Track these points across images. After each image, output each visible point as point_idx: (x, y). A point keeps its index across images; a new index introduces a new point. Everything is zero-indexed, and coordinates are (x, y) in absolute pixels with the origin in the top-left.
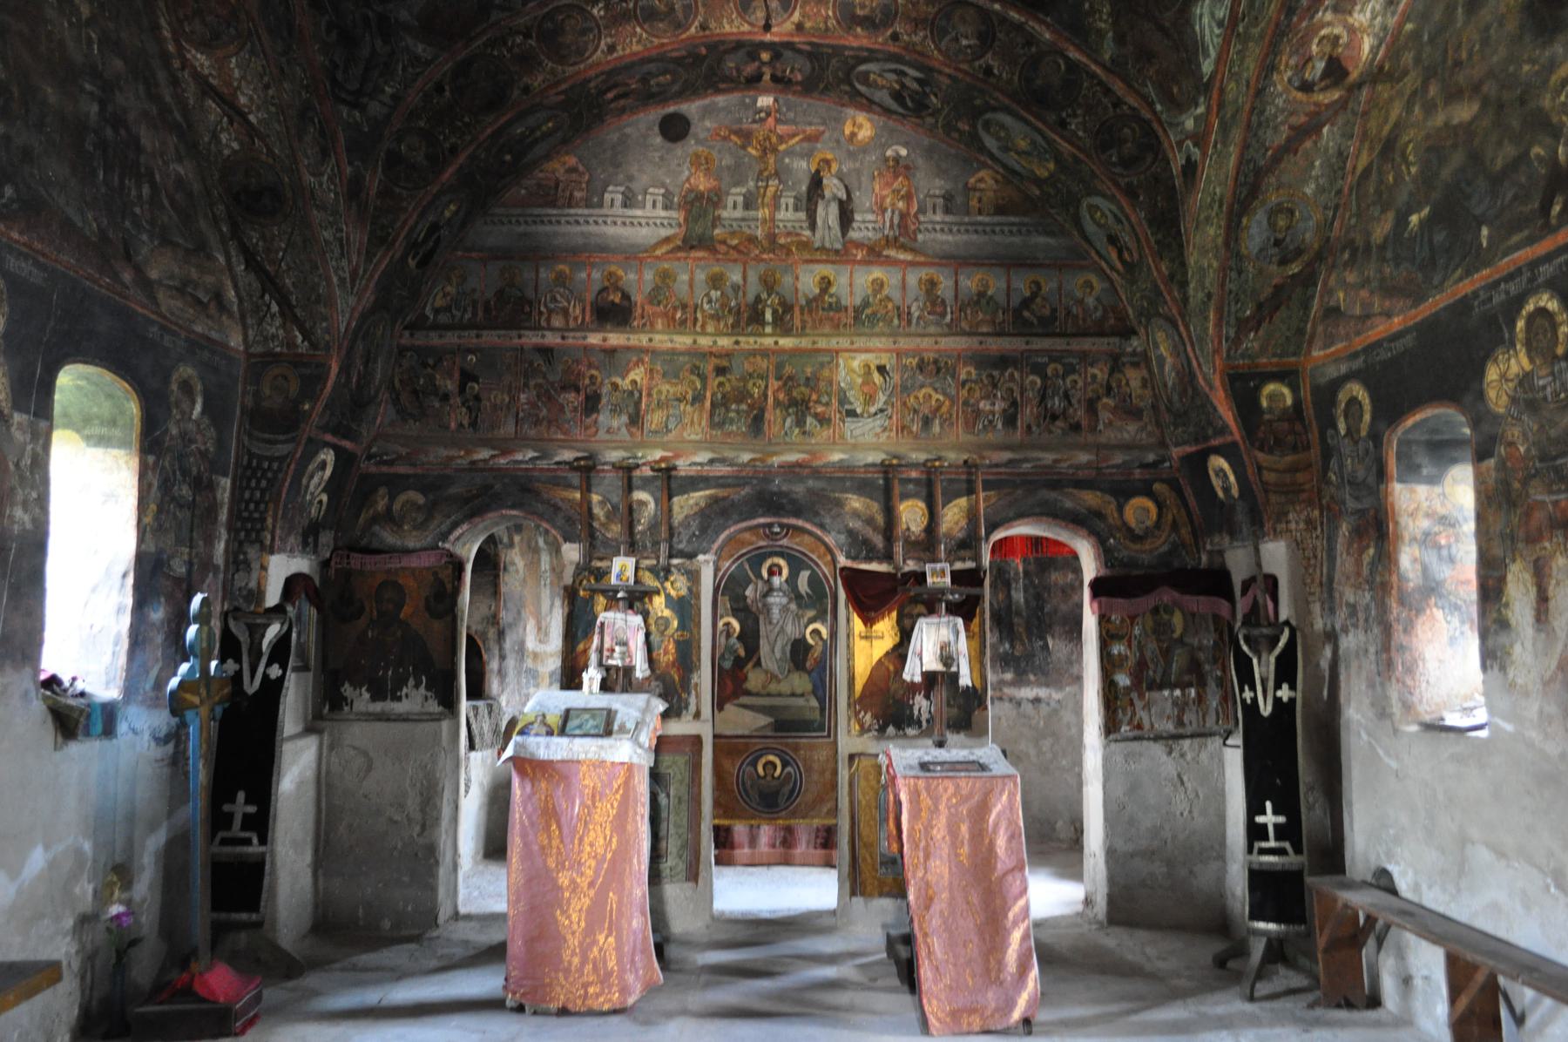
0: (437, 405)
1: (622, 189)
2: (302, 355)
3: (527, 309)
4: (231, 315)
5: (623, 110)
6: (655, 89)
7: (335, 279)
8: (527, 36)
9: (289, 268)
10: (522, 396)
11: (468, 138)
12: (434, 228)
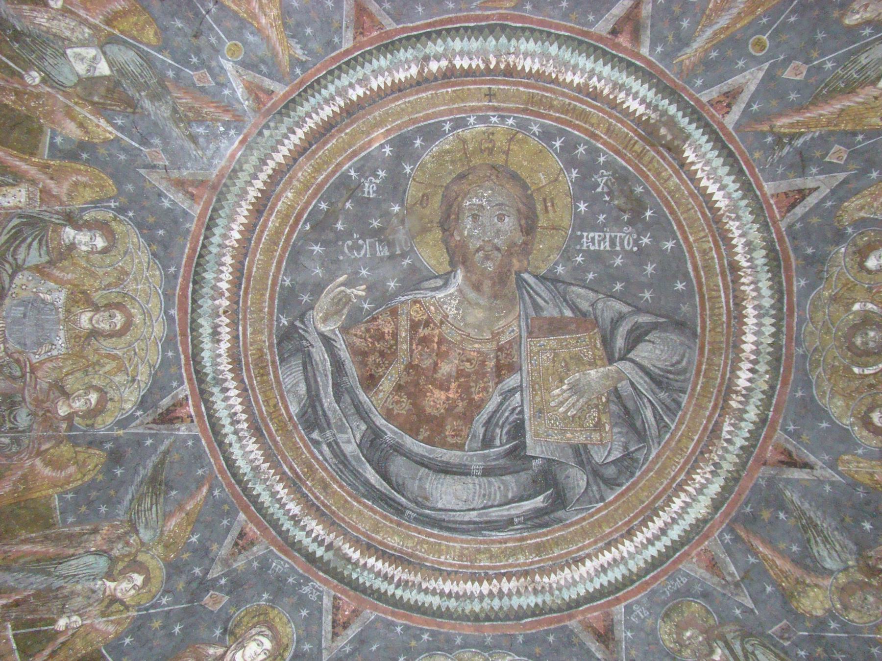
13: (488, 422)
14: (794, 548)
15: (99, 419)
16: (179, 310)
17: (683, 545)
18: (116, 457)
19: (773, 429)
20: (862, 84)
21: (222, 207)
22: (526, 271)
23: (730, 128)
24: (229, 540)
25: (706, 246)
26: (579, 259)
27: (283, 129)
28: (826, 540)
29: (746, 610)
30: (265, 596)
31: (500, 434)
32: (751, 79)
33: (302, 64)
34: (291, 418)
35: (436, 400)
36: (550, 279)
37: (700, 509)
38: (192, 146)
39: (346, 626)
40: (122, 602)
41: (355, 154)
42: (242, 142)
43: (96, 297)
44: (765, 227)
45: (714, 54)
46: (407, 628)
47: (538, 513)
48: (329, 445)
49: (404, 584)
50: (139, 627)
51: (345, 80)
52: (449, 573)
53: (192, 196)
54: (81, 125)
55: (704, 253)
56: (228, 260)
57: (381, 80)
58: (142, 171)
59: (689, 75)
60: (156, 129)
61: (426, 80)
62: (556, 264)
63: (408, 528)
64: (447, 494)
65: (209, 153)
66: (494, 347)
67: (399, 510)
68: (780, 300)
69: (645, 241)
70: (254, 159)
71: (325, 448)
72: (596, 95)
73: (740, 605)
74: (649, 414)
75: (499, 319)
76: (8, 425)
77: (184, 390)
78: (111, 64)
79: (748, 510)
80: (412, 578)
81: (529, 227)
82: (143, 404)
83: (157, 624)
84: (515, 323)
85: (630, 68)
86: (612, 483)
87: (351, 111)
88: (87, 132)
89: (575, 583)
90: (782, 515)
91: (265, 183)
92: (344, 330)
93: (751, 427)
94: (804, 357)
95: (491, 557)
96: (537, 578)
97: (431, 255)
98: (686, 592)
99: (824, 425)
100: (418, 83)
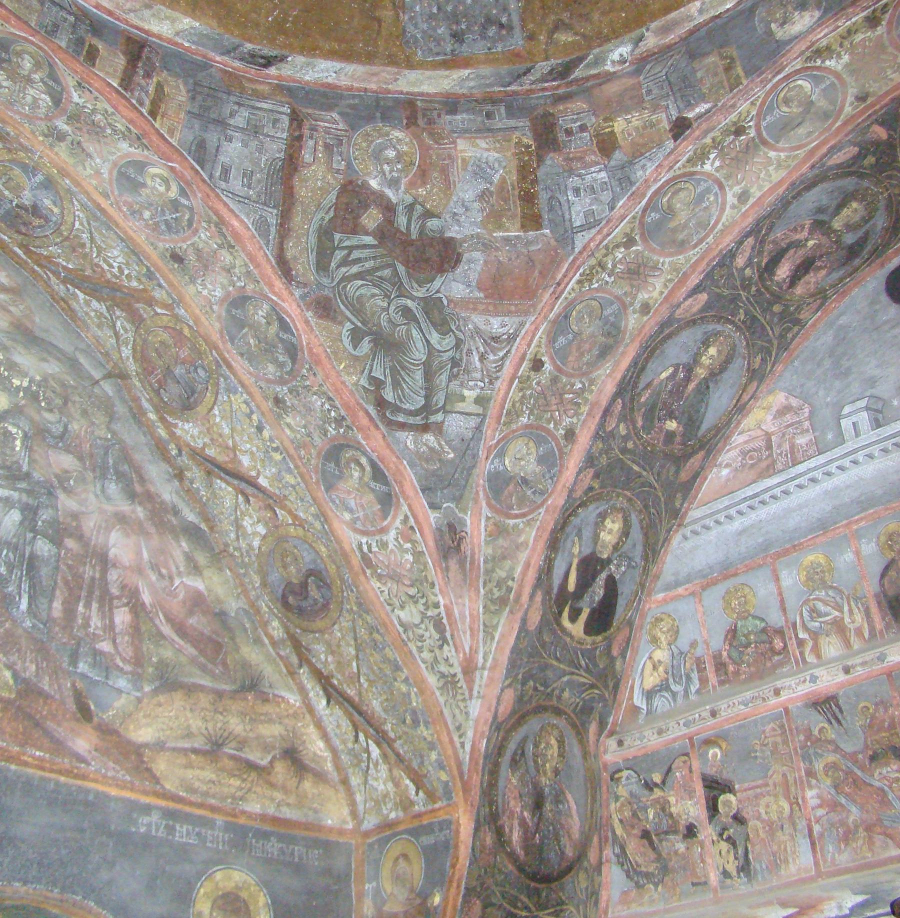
0: (681, 847)
1: (863, 403)
2: (419, 815)
3: (778, 644)
4: (320, 777)
5: (821, 296)
6: (849, 239)
7: (432, 680)
8: (630, 242)
9: (371, 682)
10: (810, 794)
11: (585, 409)
12: (590, 566)
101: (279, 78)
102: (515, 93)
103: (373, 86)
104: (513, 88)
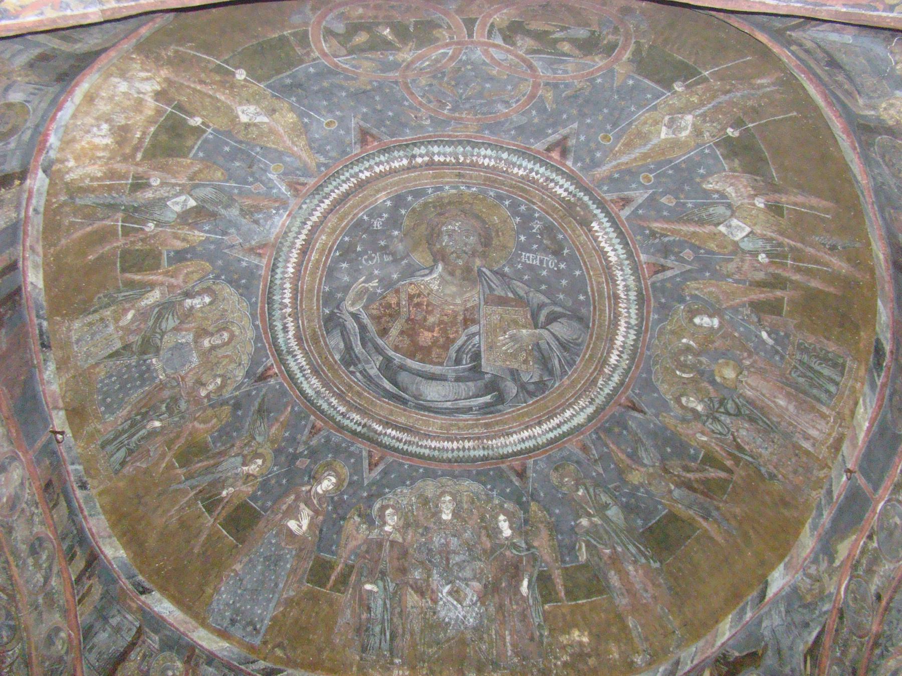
13: (458, 351)
14: (629, 450)
15: (224, 390)
16: (261, 321)
17: (569, 435)
18: (237, 406)
19: (627, 389)
20: (710, 223)
21: (280, 256)
22: (484, 266)
23: (623, 218)
24: (306, 431)
25: (600, 280)
26: (519, 266)
27: (316, 202)
28: (646, 450)
29: (598, 474)
30: (330, 456)
31: (466, 359)
32: (640, 196)
33: (325, 165)
34: (336, 362)
35: (425, 338)
36: (500, 274)
37: (581, 419)
38: (256, 226)
39: (376, 465)
40: (253, 475)
41: (366, 207)
42: (288, 215)
43: (210, 329)
44: (638, 280)
45: (616, 176)
46: (410, 466)
47: (487, 405)
48: (361, 372)
49: (409, 443)
50: (264, 485)
51: (356, 169)
52: (434, 437)
53: (260, 255)
54: (184, 240)
55: (599, 283)
56: (288, 285)
57: (381, 168)
58: (226, 251)
59: (600, 183)
60: (230, 223)
61: (414, 167)
62: (504, 265)
63: (410, 412)
64: (433, 392)
65: (267, 227)
66: (463, 308)
67: (404, 402)
68: (641, 322)
69: (562, 266)
70: (298, 223)
71: (358, 374)
72: (534, 181)
73: (596, 471)
74: (556, 362)
75: (466, 292)
76: (176, 411)
77: (271, 360)
78: (196, 199)
79: (607, 425)
80: (413, 439)
81: (486, 242)
82: (247, 375)
83: (273, 482)
84: (476, 296)
85: (557, 170)
86: (531, 394)
87: (361, 185)
88: (188, 242)
89: (506, 446)
90: (625, 432)
91: (306, 235)
92: (366, 307)
93: (614, 385)
94: (650, 356)
95: (459, 428)
96: (485, 441)
97: (420, 258)
98: (567, 459)
99: (656, 395)
100: (408, 168)
101: (144, 603)
102: (241, 670)
103: (182, 629)
104: (243, 667)
